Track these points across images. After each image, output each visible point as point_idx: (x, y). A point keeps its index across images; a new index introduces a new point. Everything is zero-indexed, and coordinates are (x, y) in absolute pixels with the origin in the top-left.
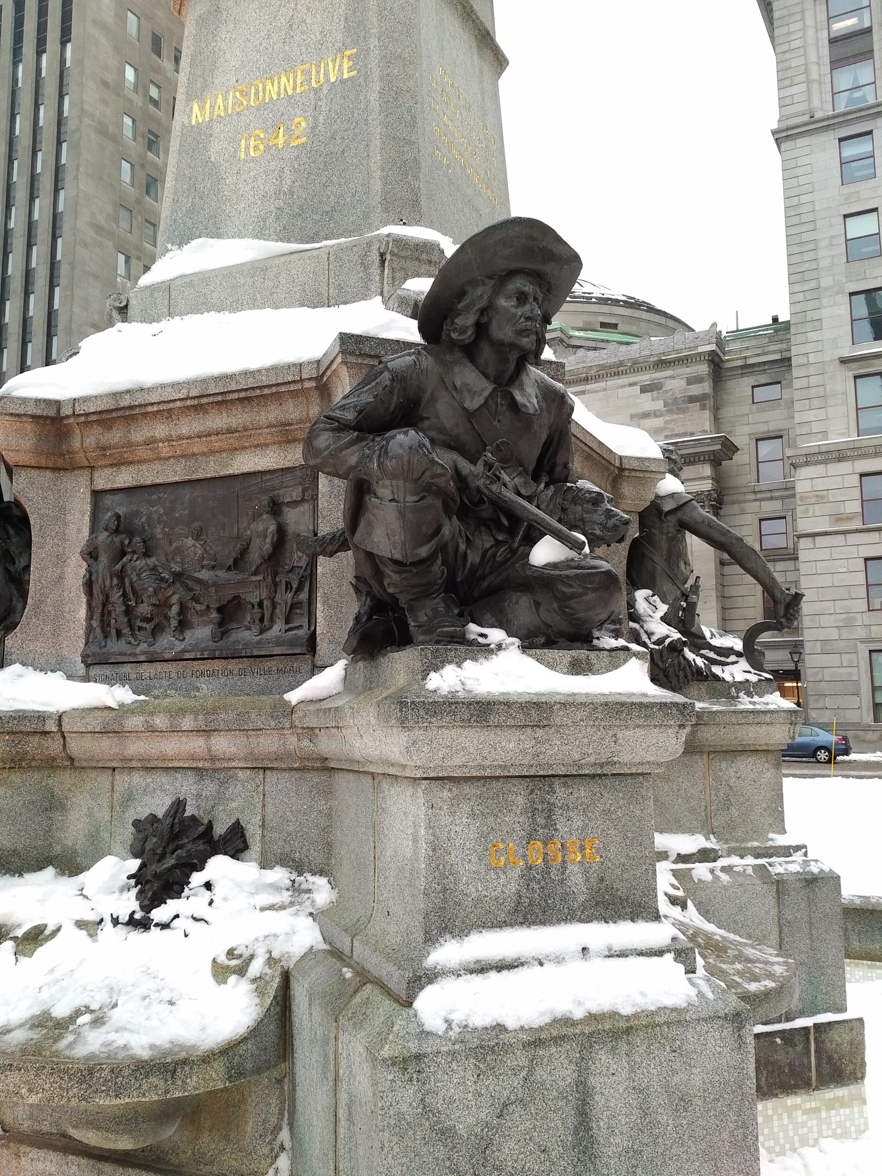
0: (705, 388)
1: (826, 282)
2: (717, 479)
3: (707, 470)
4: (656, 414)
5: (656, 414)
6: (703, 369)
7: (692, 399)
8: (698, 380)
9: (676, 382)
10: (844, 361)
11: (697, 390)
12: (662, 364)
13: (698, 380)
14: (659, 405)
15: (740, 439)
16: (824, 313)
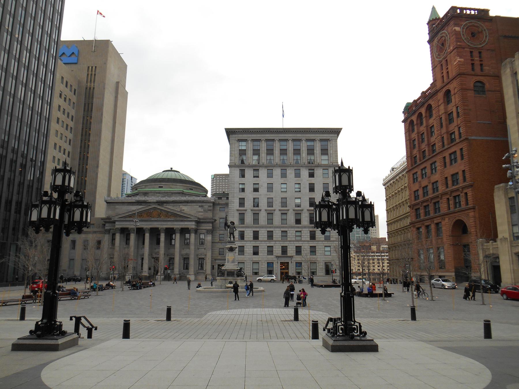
0: (211, 208)
1: (235, 195)
2: (213, 227)
3: (211, 225)
4: (202, 212)
5: (202, 212)
6: (212, 204)
7: (209, 210)
8: (210, 206)
9: (206, 206)
10: (237, 210)
11: (210, 208)
12: (203, 202)
13: (210, 206)
14: (202, 210)
15: (217, 218)
16: (235, 201)
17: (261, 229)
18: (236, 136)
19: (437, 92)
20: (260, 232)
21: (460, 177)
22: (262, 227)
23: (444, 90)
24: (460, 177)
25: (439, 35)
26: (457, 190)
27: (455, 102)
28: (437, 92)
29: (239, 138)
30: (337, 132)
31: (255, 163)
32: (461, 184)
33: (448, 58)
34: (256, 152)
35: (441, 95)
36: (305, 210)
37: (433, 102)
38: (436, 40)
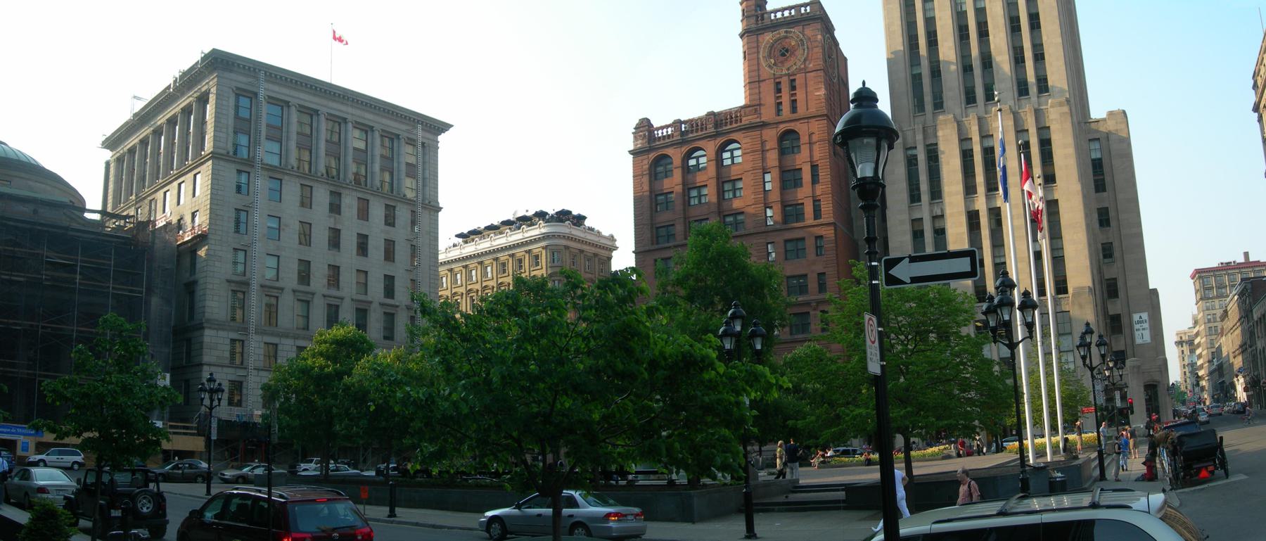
17: (284, 341)
18: (233, 76)
19: (764, 125)
20: (280, 347)
21: (813, 284)
22: (286, 335)
23: (783, 127)
24: (813, 284)
25: (782, 32)
26: (808, 304)
27: (811, 156)
28: (764, 125)
29: (240, 85)
30: (442, 127)
31: (274, 161)
32: (813, 295)
33: (799, 79)
34: (277, 134)
35: (771, 135)
36: (375, 306)
37: (748, 140)
38: (768, 37)
